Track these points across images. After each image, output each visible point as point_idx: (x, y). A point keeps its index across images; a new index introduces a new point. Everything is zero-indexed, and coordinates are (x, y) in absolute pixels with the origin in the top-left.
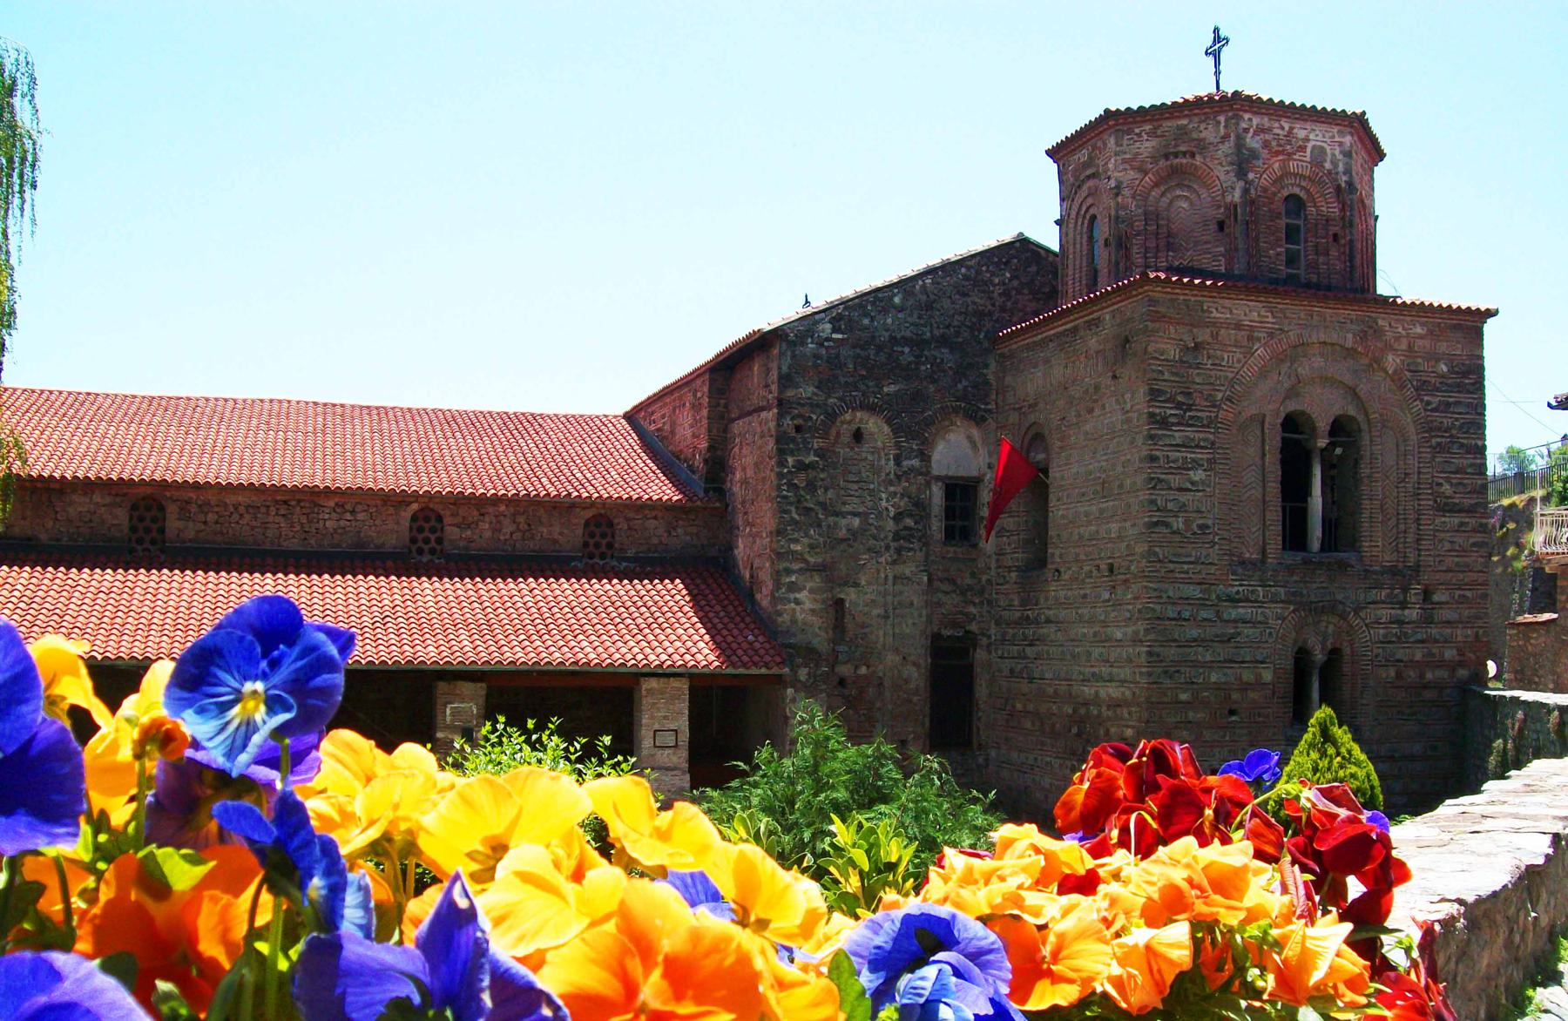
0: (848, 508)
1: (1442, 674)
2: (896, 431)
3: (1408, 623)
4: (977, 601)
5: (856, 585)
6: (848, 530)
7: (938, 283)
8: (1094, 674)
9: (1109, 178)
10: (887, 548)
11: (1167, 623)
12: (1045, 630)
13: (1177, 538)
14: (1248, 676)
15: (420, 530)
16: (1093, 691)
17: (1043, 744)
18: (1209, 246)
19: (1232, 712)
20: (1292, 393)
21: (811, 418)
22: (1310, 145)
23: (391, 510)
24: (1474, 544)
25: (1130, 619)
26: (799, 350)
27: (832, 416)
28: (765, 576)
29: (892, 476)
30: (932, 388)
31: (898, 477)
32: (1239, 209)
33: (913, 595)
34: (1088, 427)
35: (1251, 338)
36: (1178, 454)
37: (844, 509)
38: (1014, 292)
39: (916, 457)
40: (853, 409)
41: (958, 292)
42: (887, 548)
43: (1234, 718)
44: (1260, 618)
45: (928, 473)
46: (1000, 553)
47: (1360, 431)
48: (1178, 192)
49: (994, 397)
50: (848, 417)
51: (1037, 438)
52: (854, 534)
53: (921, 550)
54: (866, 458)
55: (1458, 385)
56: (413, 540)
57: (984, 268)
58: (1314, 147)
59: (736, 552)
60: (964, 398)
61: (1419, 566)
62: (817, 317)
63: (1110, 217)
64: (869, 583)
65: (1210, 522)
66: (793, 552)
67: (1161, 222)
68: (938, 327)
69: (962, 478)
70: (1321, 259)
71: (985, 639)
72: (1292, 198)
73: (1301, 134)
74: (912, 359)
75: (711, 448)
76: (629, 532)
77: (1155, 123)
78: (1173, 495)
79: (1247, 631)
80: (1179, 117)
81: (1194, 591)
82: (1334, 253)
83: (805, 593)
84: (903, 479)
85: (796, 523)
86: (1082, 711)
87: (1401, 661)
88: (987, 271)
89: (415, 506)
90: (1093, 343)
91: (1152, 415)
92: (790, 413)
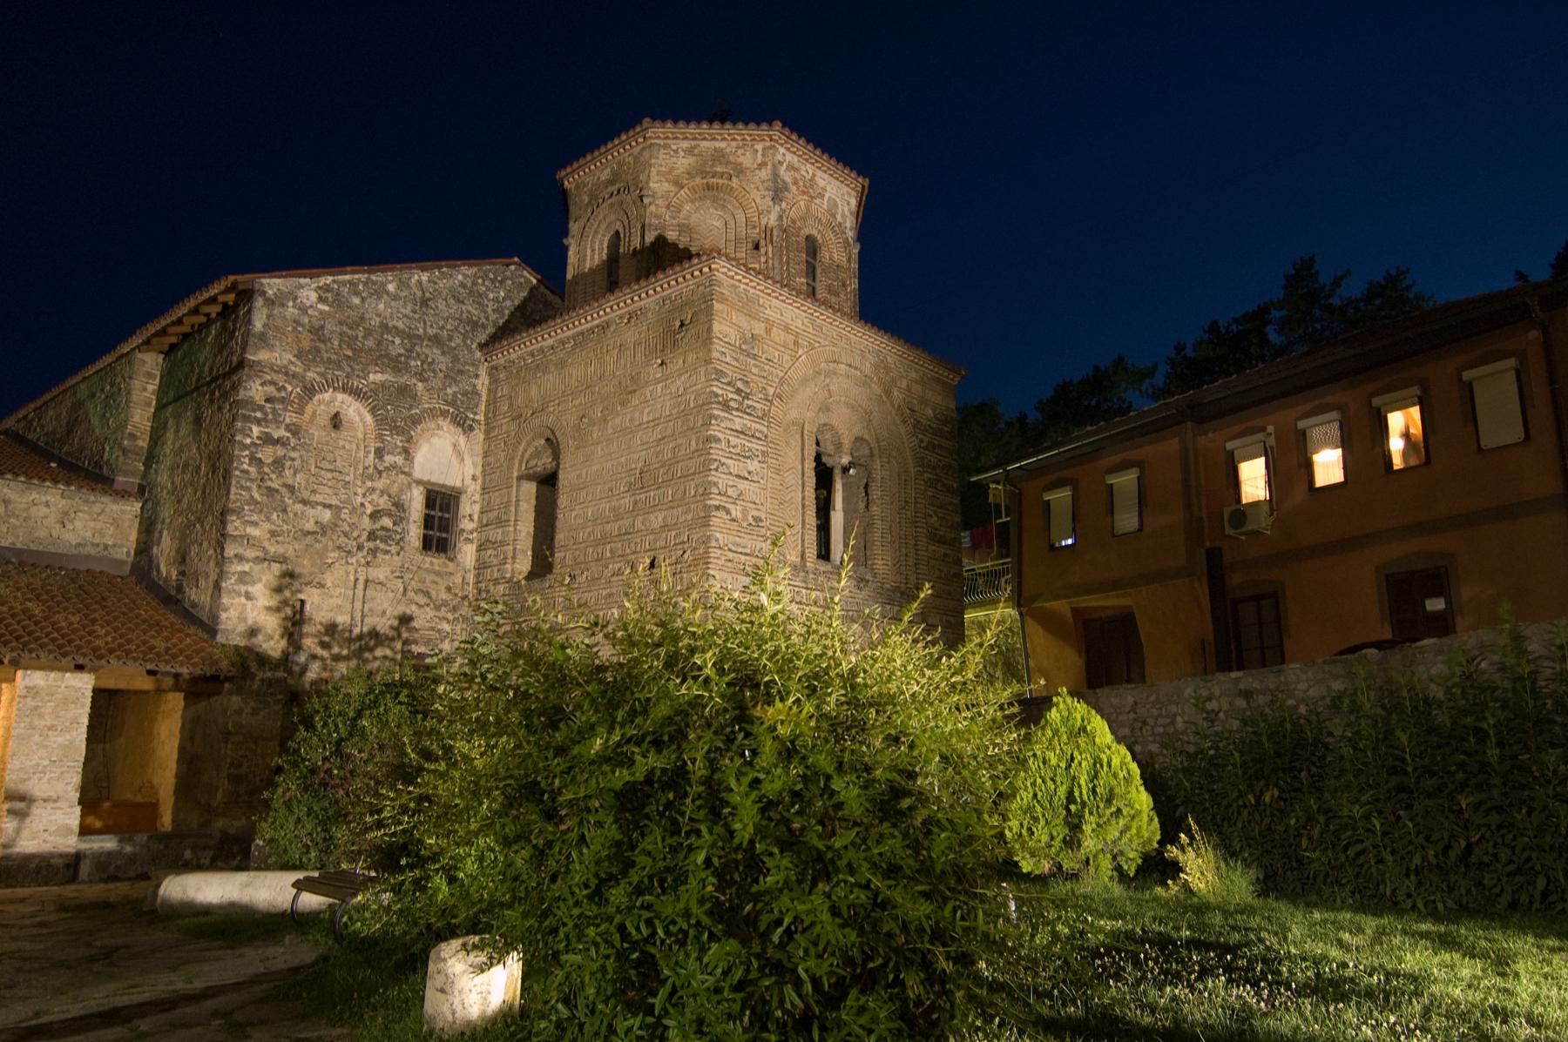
0: (318, 498)
2: (380, 421)
4: (450, 616)
5: (321, 585)
6: (317, 522)
10: (360, 548)
13: (735, 526)
20: (825, 409)
21: (284, 388)
22: (827, 195)
27: (310, 391)
29: (371, 470)
30: (420, 386)
31: (380, 473)
32: (775, 233)
35: (796, 343)
36: (739, 441)
37: (313, 498)
39: (400, 453)
40: (334, 389)
41: (454, 297)
42: (360, 548)
46: (481, 566)
50: (327, 396)
52: (323, 529)
53: (398, 554)
54: (344, 447)
57: (480, 281)
58: (829, 198)
60: (453, 403)
65: (763, 516)
69: (443, 486)
73: (821, 183)
74: (402, 351)
77: (694, 143)
84: (384, 475)
85: (257, 503)
88: (483, 284)
92: (261, 377)
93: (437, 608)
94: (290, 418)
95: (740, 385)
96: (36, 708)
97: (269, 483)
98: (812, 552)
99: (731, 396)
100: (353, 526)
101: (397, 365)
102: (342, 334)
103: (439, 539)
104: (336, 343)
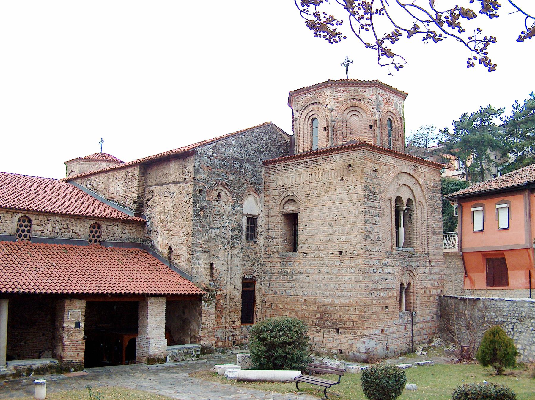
0: (216, 226)
1: (434, 291)
3: (427, 273)
4: (256, 264)
7: (247, 138)
9: (326, 105)
10: (229, 242)
11: (370, 274)
13: (372, 242)
14: (390, 294)
15: (21, 226)
16: (330, 301)
18: (366, 134)
19: (387, 307)
22: (394, 102)
24: (441, 246)
27: (212, 187)
28: (183, 251)
29: (231, 213)
32: (378, 122)
33: (237, 261)
34: (326, 198)
35: (389, 169)
36: (372, 210)
38: (269, 144)
42: (229, 242)
43: (387, 310)
44: (393, 272)
47: (413, 204)
48: (354, 113)
49: (263, 184)
50: (217, 188)
55: (435, 190)
56: (18, 231)
57: (261, 134)
59: (155, 242)
61: (428, 253)
62: (208, 146)
64: (222, 256)
65: (380, 236)
67: (347, 123)
68: (246, 155)
70: (397, 143)
71: (259, 279)
72: (389, 119)
73: (392, 98)
74: (238, 167)
75: (138, 197)
76: (107, 231)
77: (346, 87)
78: (371, 225)
79: (390, 277)
80: (355, 86)
81: (376, 262)
83: (202, 260)
85: (199, 231)
86: (323, 308)
87: (425, 287)
89: (20, 215)
90: (328, 166)
91: (365, 195)
95: (372, 189)
96: (153, 308)
97: (203, 223)
98: (394, 246)
99: (370, 194)
101: (236, 171)
103: (251, 234)
104: (219, 167)
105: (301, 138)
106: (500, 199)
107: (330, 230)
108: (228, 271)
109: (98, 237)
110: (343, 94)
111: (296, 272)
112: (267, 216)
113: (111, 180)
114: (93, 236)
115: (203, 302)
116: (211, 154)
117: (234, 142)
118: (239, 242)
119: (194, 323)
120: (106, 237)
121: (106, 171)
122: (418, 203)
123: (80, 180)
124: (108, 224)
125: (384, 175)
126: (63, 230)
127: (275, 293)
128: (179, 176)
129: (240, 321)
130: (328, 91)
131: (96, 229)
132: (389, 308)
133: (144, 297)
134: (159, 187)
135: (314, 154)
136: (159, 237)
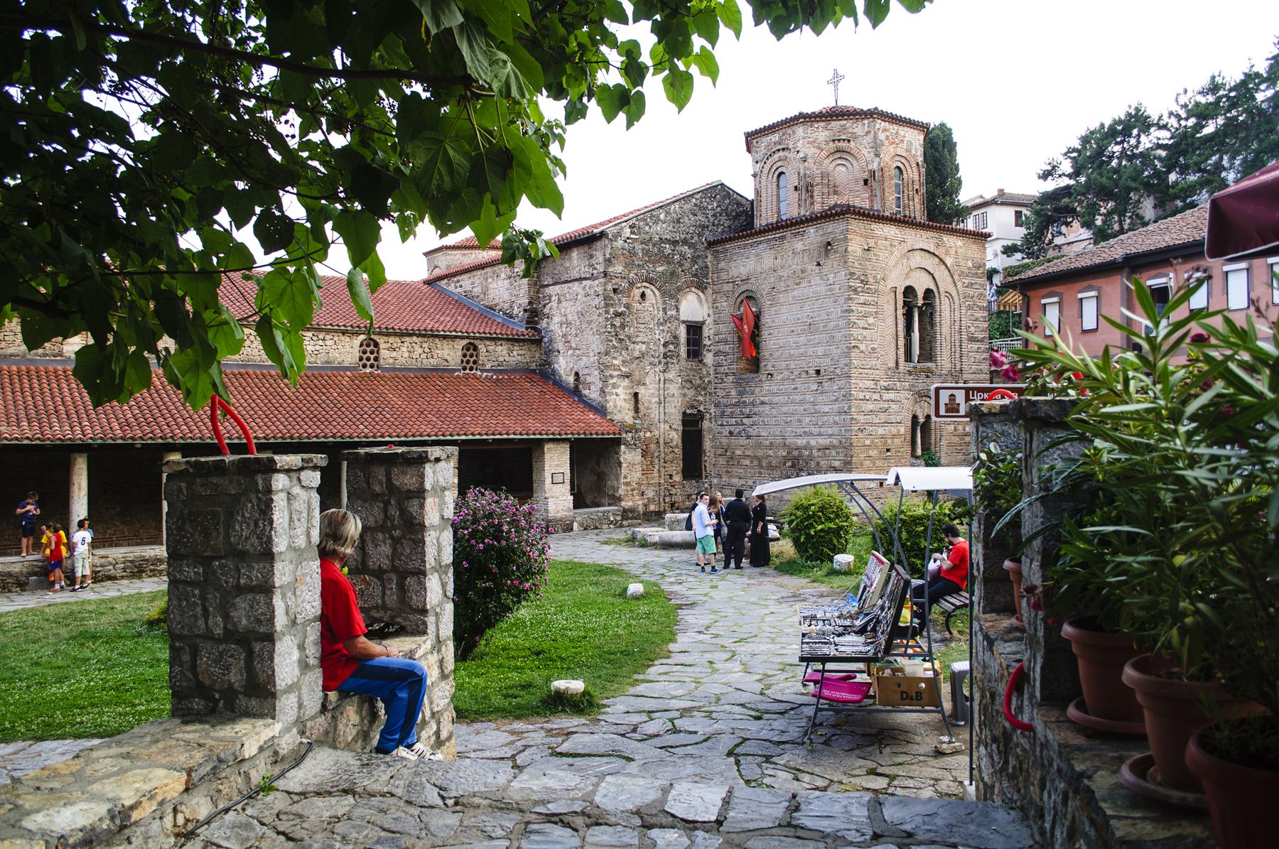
0: (638, 339)
2: (663, 294)
5: (645, 384)
8: (805, 433)
10: (660, 363)
12: (761, 409)
13: (862, 355)
14: (894, 430)
15: (364, 352)
16: (804, 441)
17: (760, 473)
23: (348, 339)
25: (836, 400)
26: (615, 244)
27: (632, 284)
28: (593, 378)
33: (673, 389)
34: (795, 293)
35: (891, 245)
45: (678, 319)
46: (718, 365)
48: (840, 162)
50: (639, 285)
51: (750, 297)
52: (643, 355)
55: (976, 274)
56: (361, 359)
60: (695, 275)
63: (799, 173)
66: (614, 365)
72: (898, 168)
73: (902, 133)
75: (530, 303)
78: (861, 331)
81: (870, 384)
82: (916, 200)
83: (621, 389)
85: (615, 347)
86: (795, 453)
89: (363, 337)
90: (799, 246)
91: (851, 287)
93: (696, 389)
94: (624, 300)
98: (902, 360)
100: (655, 351)
101: (668, 259)
102: (643, 249)
105: (763, 204)
106: (1085, 284)
107: (802, 339)
108: (660, 403)
109: (475, 362)
110: (821, 133)
111: (758, 402)
112: (716, 322)
113: (490, 280)
114: (468, 362)
115: (623, 447)
116: (628, 235)
117: (662, 217)
118: (675, 361)
119: (612, 477)
120: (486, 362)
121: (482, 267)
122: (943, 294)
123: (446, 281)
124: (488, 343)
125: (883, 255)
126: (424, 356)
127: (731, 433)
128: (584, 270)
129: (680, 475)
130: (800, 130)
131: (471, 351)
132: (893, 451)
133: (539, 444)
134: (557, 287)
135: (782, 227)
136: (561, 359)
